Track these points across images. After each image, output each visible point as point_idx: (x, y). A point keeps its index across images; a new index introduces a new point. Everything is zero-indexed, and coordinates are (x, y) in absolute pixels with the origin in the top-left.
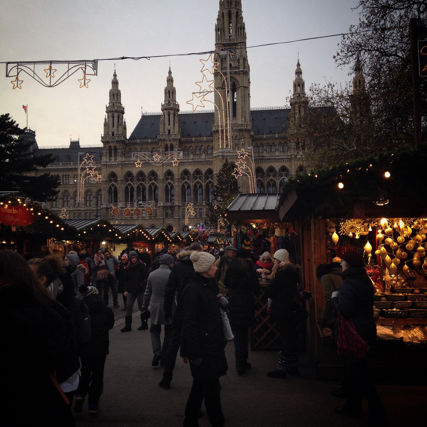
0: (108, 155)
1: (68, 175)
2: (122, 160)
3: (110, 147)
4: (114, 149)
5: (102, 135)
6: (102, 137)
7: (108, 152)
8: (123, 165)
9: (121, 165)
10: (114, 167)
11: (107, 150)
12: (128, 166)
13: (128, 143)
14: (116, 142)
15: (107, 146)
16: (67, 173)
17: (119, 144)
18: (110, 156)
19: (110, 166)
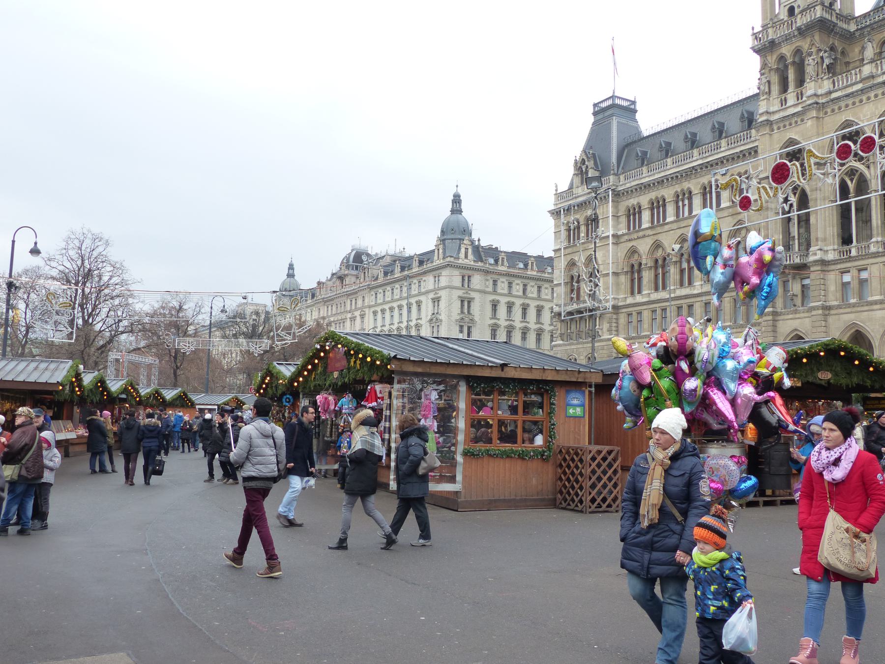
0: (775, 89)
1: (689, 188)
2: (820, 92)
3: (782, 58)
4: (794, 63)
5: (753, 28)
6: (754, 34)
7: (775, 79)
8: (821, 107)
9: (818, 110)
10: (796, 122)
11: (773, 73)
12: (843, 104)
13: (857, 30)
14: (800, 33)
15: (772, 60)
16: (686, 185)
17: (808, 40)
18: (784, 88)
19: (782, 125)
